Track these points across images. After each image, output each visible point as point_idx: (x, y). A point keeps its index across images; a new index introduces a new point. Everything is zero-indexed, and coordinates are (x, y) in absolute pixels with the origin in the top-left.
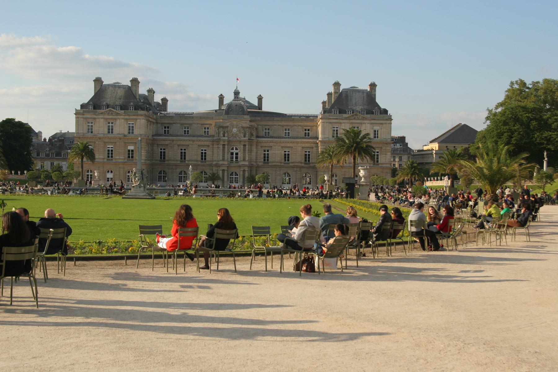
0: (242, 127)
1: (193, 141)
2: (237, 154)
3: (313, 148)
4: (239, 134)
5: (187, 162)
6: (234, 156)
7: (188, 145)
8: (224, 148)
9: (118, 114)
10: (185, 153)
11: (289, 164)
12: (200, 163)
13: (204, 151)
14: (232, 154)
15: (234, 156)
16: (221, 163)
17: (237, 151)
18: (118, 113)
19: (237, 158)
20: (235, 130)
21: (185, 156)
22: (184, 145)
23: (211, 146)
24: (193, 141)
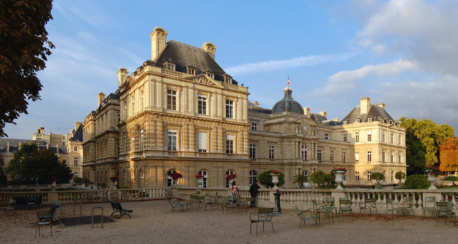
0: (310, 125)
1: (264, 136)
2: (306, 152)
3: (347, 149)
4: (309, 133)
5: (257, 160)
6: (304, 154)
7: (258, 141)
8: (299, 145)
9: (213, 86)
10: (254, 149)
11: (334, 162)
12: (269, 161)
13: (271, 149)
14: (303, 152)
15: (304, 154)
16: (298, 161)
17: (306, 150)
18: (214, 84)
19: (306, 156)
20: (305, 128)
21: (254, 153)
22: (254, 141)
23: (279, 143)
24: (264, 136)
